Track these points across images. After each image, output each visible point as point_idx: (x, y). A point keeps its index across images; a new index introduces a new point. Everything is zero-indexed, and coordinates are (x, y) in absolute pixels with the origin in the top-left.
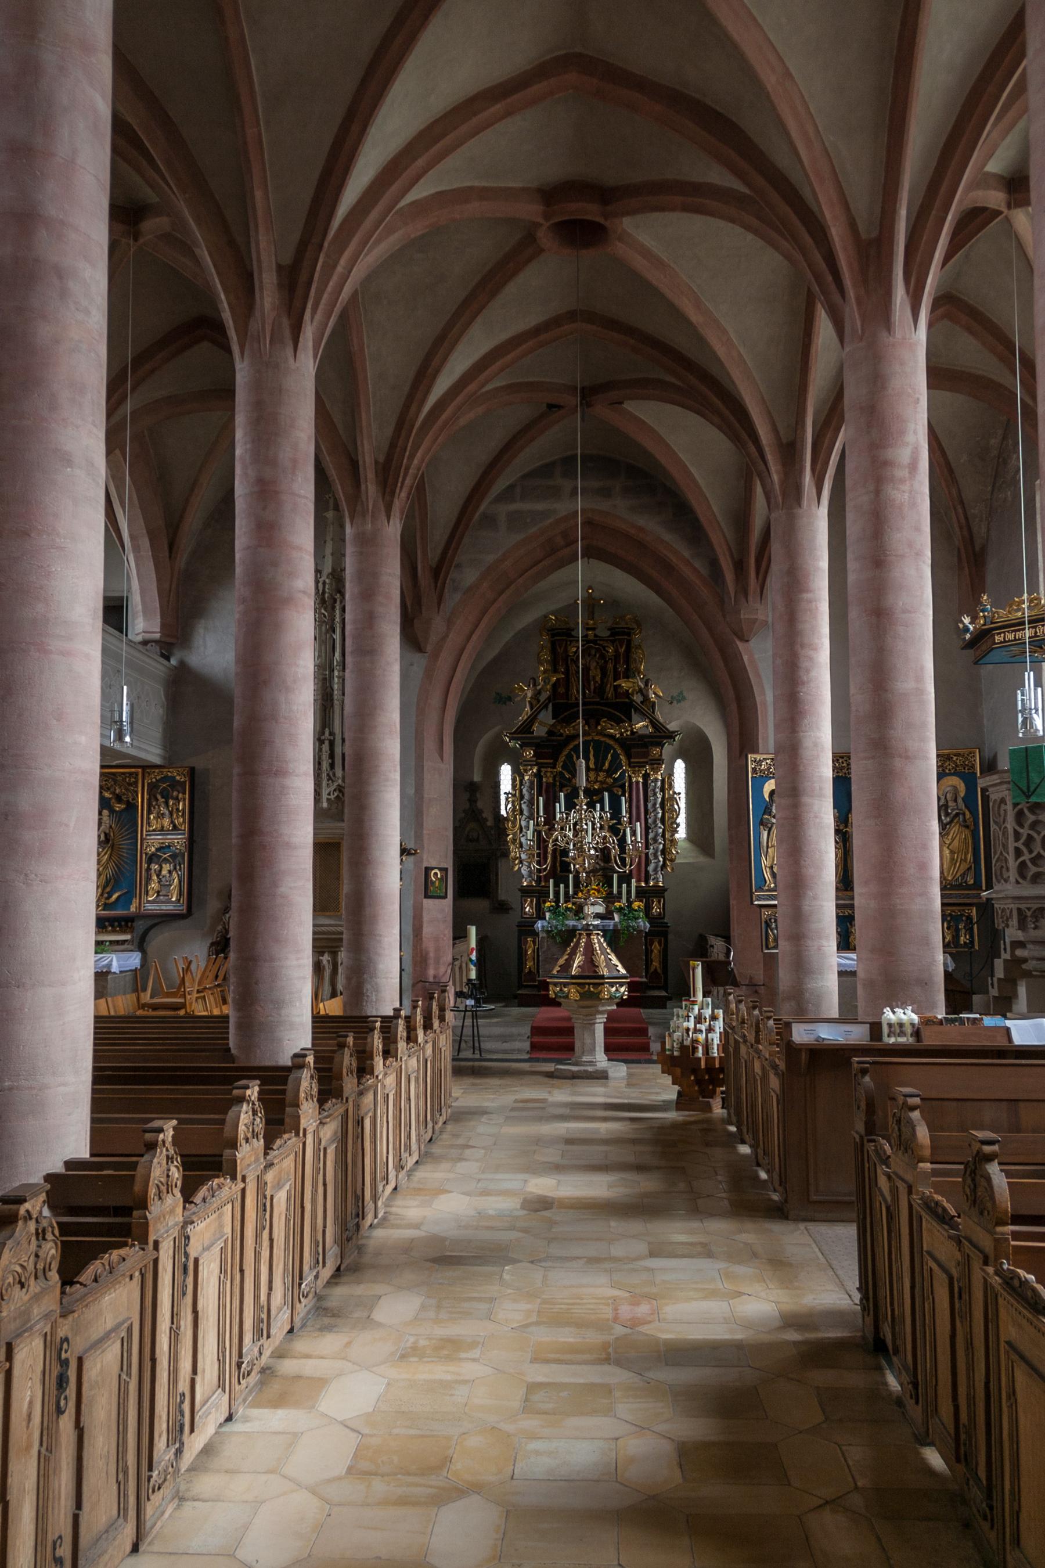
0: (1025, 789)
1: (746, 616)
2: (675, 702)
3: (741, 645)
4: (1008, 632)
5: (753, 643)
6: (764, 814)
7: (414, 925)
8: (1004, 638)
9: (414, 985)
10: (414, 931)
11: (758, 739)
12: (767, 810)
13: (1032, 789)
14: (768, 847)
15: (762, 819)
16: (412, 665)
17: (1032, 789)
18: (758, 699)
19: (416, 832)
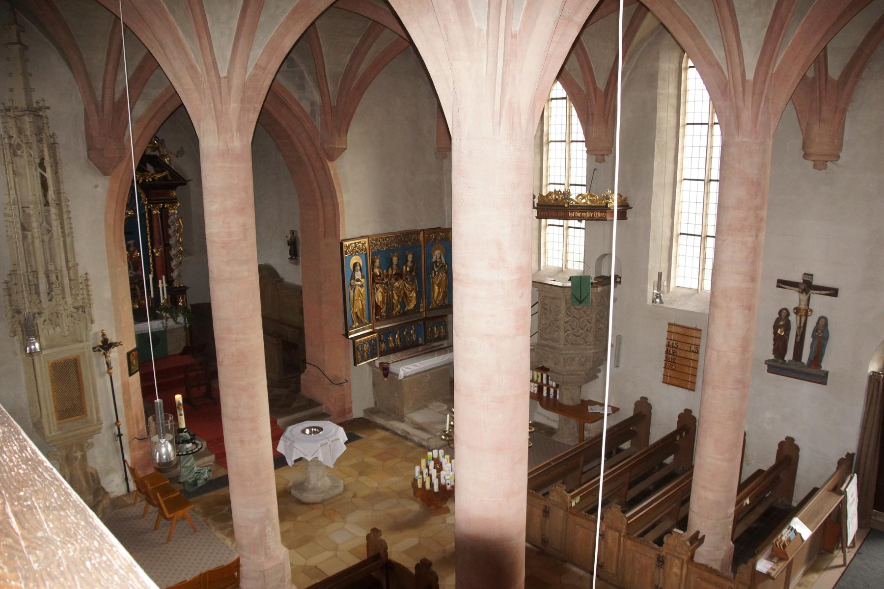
0: (579, 299)
1: (339, 147)
2: (179, 155)
3: (329, 164)
4: (577, 212)
5: (335, 162)
6: (351, 280)
7: (124, 399)
8: (575, 215)
9: (130, 443)
10: (124, 403)
11: (339, 227)
12: (353, 277)
13: (582, 299)
14: (354, 300)
15: (350, 283)
16: (96, 186)
17: (582, 299)
18: (339, 200)
19: (116, 328)
